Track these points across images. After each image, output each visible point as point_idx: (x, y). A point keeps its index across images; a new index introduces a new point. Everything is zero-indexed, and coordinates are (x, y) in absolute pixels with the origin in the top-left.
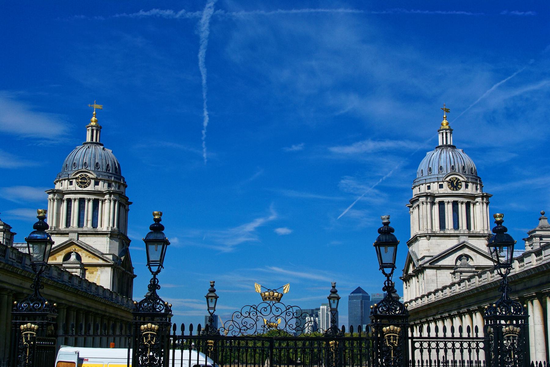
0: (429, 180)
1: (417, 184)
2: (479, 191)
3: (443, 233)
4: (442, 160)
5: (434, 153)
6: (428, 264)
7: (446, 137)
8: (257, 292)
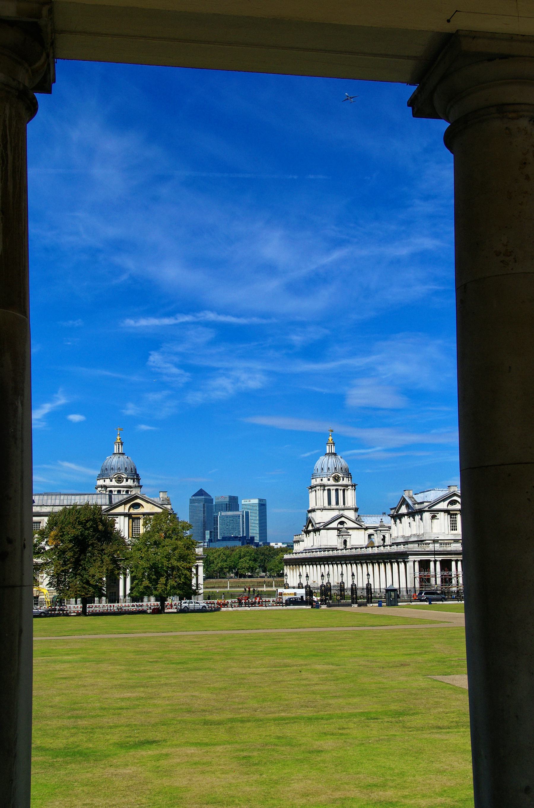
2: (350, 481)
4: (329, 463)
6: (322, 527)
7: (331, 448)
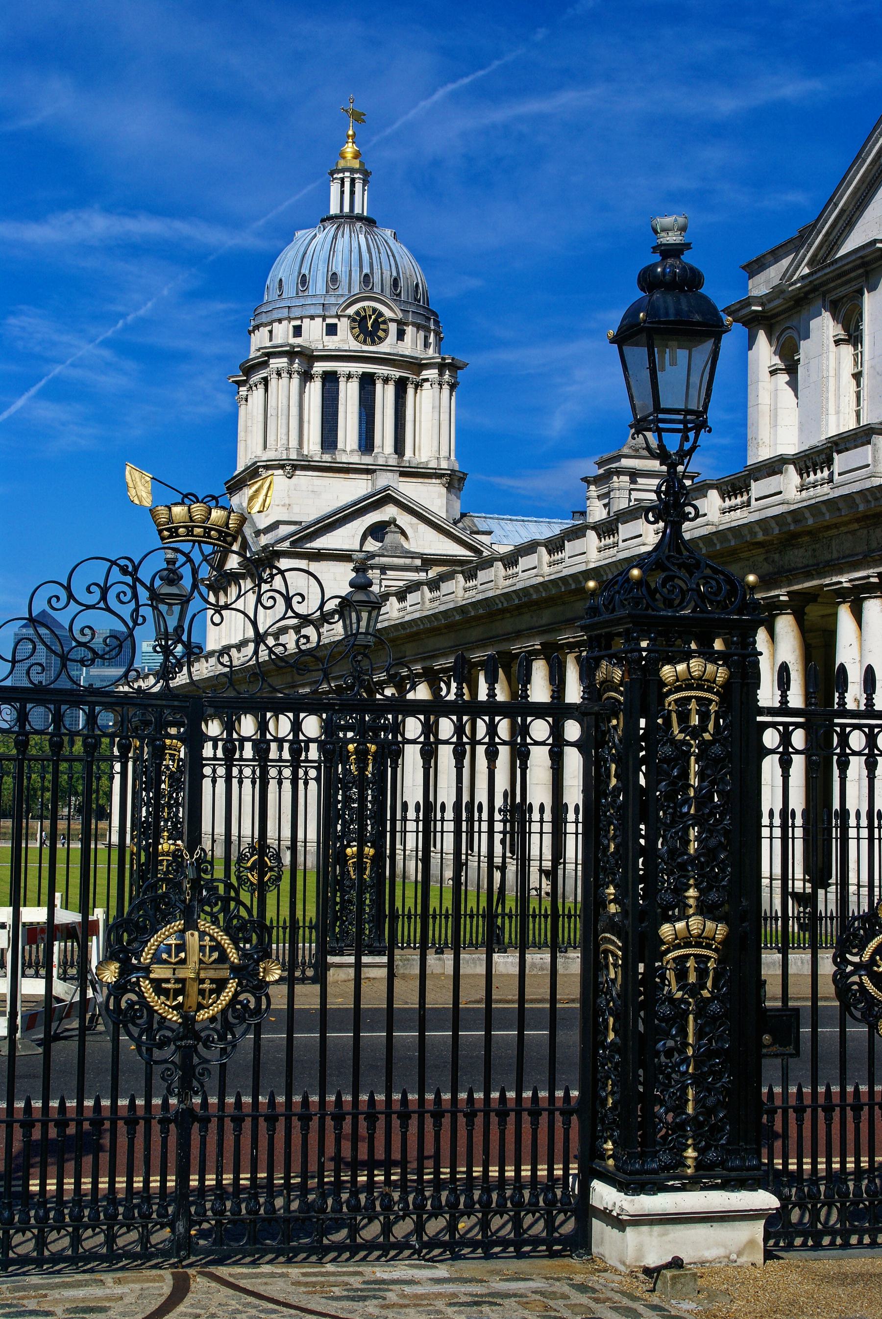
0: (300, 309)
1: (264, 319)
2: (431, 352)
3: (330, 460)
5: (315, 235)
7: (352, 193)
8: (137, 502)
